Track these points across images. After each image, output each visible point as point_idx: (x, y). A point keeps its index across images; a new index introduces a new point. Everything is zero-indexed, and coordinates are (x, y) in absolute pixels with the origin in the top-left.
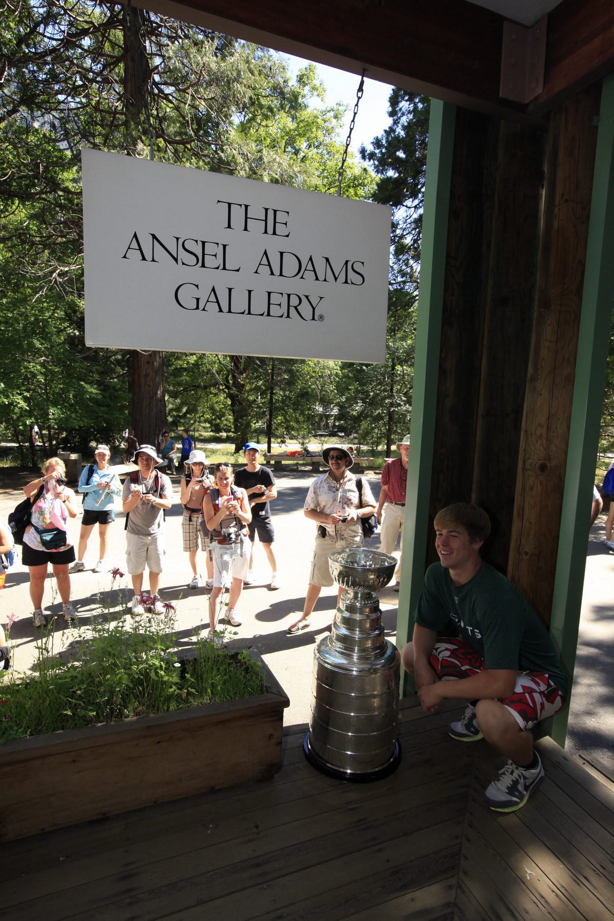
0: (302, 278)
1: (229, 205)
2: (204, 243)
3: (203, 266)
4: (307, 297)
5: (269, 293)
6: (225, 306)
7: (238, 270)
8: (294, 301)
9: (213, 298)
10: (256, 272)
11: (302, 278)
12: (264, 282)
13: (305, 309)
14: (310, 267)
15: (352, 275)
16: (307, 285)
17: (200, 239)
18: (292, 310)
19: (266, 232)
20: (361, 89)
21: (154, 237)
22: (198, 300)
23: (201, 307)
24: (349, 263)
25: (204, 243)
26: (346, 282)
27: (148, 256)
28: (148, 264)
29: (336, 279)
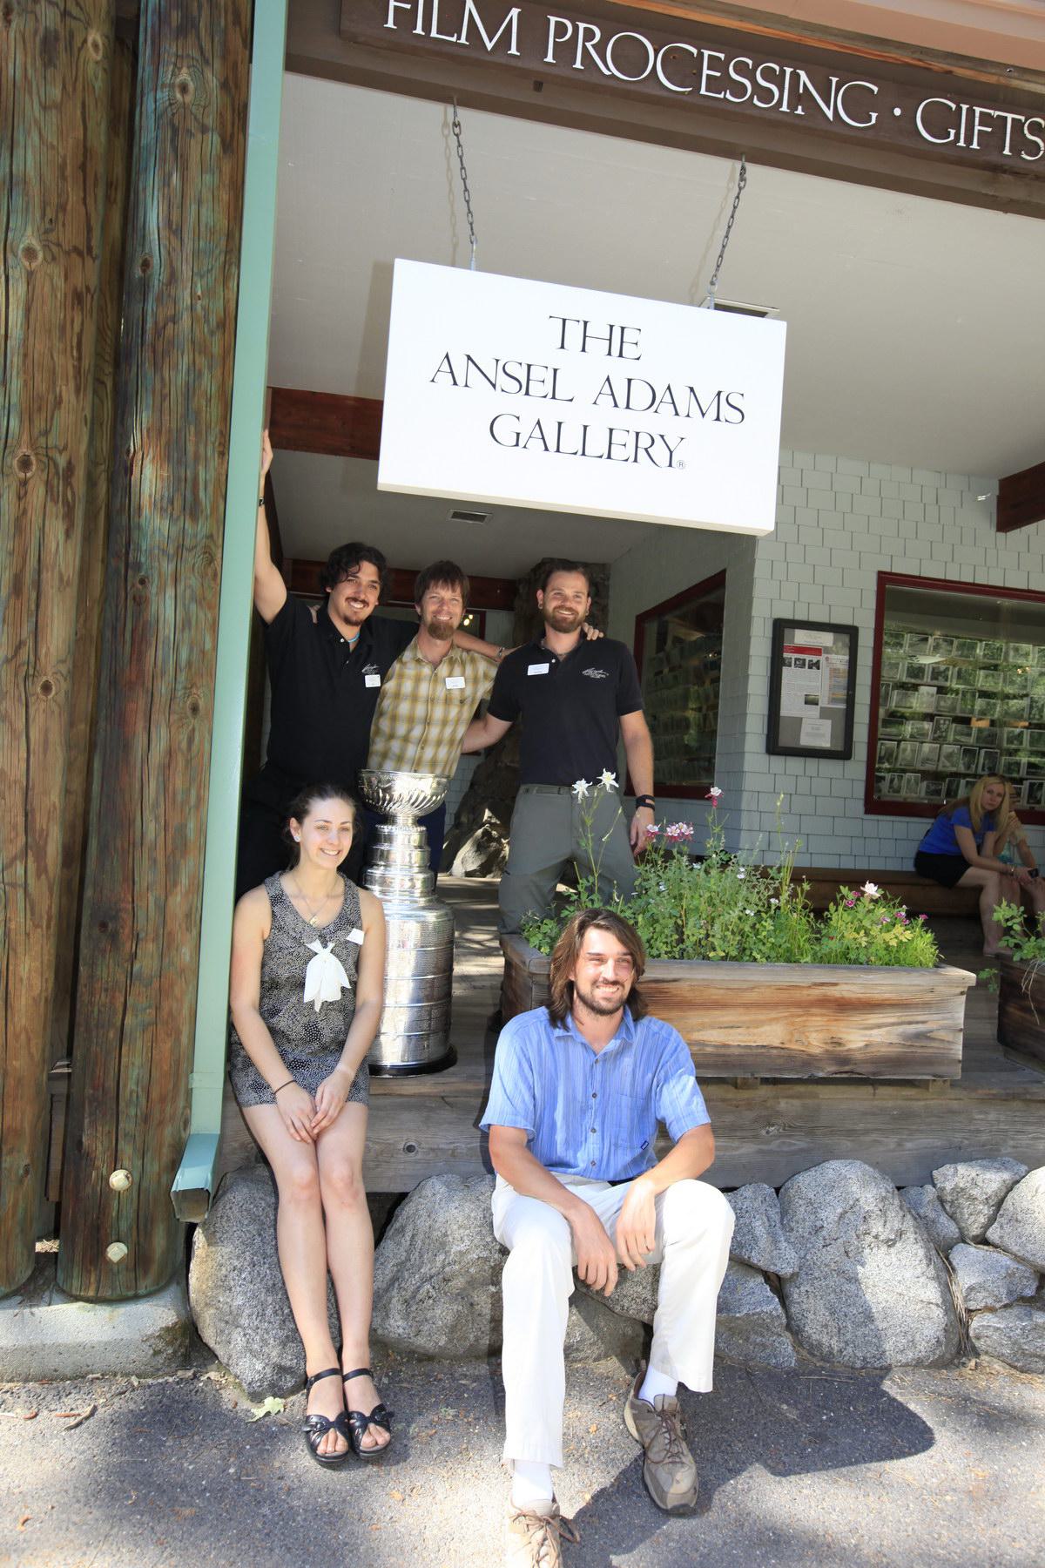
1: (564, 320)
2: (529, 366)
3: (527, 393)
4: (662, 436)
5: (611, 430)
7: (571, 400)
9: (537, 433)
12: (604, 416)
13: (659, 452)
14: (668, 398)
15: (726, 411)
16: (661, 422)
17: (525, 361)
18: (641, 453)
19: (609, 354)
20: (742, 179)
21: (469, 358)
22: (518, 434)
23: (522, 443)
25: (529, 366)
26: (718, 419)
27: (461, 380)
28: (460, 388)
29: (703, 415)
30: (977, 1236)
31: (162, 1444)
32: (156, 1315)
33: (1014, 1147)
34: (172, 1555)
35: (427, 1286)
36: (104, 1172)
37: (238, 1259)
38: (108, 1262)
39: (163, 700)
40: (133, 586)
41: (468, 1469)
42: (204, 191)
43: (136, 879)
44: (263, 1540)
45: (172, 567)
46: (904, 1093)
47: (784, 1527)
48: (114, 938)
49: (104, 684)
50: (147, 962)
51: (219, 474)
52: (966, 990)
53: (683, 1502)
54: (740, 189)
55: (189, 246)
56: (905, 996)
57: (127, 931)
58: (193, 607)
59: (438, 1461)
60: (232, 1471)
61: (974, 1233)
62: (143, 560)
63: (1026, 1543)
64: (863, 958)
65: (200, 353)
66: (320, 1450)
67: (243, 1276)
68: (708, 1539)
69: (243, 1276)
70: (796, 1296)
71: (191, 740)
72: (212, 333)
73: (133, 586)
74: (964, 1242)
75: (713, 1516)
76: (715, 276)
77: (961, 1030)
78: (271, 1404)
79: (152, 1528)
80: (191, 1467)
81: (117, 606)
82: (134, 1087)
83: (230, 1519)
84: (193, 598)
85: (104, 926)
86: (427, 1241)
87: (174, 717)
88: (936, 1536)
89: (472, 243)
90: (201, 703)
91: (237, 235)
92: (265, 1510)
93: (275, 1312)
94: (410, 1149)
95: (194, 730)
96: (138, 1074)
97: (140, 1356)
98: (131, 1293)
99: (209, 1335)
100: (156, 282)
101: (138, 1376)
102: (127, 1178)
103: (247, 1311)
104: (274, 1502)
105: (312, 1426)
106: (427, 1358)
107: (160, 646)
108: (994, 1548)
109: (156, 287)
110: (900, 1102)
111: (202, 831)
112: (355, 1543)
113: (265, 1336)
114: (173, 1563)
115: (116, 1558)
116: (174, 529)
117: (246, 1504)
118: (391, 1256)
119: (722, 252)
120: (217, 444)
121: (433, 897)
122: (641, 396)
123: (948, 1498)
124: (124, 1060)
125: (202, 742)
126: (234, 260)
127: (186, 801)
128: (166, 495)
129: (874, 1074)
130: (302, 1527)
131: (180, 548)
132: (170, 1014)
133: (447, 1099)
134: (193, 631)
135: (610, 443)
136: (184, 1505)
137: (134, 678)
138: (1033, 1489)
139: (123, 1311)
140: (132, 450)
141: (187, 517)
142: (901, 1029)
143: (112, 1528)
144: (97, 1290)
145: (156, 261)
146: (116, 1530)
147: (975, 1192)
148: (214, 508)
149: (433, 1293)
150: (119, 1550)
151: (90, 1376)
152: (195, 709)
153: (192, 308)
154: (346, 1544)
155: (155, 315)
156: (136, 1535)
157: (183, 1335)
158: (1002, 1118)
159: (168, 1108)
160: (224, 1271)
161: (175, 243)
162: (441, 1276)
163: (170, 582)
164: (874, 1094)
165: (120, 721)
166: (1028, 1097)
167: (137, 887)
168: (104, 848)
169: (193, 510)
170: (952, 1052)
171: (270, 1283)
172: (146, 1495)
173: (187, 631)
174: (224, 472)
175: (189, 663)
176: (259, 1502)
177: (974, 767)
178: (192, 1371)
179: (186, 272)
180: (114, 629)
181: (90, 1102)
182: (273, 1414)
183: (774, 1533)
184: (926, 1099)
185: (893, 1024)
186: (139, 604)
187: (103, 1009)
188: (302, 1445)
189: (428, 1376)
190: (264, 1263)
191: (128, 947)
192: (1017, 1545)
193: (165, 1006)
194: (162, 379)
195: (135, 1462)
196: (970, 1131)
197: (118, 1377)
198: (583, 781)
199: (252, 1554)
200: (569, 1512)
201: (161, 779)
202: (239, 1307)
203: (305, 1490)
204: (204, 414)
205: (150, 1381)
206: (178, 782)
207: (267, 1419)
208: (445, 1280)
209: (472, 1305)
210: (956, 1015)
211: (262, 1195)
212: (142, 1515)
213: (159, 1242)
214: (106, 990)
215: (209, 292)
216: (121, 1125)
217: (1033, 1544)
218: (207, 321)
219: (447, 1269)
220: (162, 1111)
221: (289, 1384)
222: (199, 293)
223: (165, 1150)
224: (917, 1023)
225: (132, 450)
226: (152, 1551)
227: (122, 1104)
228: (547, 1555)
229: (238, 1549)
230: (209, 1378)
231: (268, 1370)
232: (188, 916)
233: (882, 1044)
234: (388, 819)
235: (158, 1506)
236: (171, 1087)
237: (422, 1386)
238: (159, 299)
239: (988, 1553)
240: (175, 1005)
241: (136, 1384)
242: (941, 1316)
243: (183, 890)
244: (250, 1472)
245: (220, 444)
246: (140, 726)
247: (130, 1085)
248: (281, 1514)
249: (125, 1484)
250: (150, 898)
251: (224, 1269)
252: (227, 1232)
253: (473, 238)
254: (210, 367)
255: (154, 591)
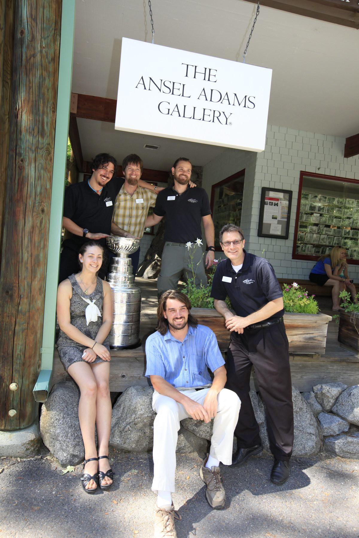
0: (222, 103)
1: (188, 65)
2: (174, 83)
3: (173, 94)
4: (224, 113)
5: (204, 109)
6: (182, 114)
7: (189, 97)
8: (217, 114)
9: (176, 109)
10: (198, 99)
11: (222, 103)
12: (202, 104)
14: (226, 98)
15: (248, 103)
16: (224, 107)
17: (172, 81)
18: (215, 118)
19: (205, 79)
20: (258, 11)
21: (151, 79)
22: (169, 110)
23: (170, 113)
24: (247, 97)
25: (174, 83)
26: (245, 106)
27: (147, 88)
28: (147, 91)
29: (239, 105)
30: (328, 410)
31: (28, 483)
32: (28, 435)
33: (342, 378)
34: (30, 524)
35: (128, 426)
36: (8, 384)
37: (58, 416)
38: (9, 417)
39: (30, 207)
40: (18, 162)
41: (142, 492)
42: (45, 2)
43: (20, 275)
44: (64, 519)
45: (33, 155)
46: (304, 359)
47: (256, 513)
48: (11, 296)
49: (7, 200)
50: (24, 306)
51: (53, 120)
52: (328, 322)
53: (220, 505)
54: (257, 15)
55: (39, 26)
56: (306, 324)
57: (16, 294)
58: (42, 171)
59: (131, 489)
60: (54, 493)
61: (327, 409)
62: (22, 152)
63: (342, 518)
64: (291, 310)
65: (44, 71)
66: (86, 488)
67: (60, 422)
68: (229, 518)
69: (60, 422)
70: (263, 431)
71: (41, 223)
72: (49, 63)
73: (18, 162)
74: (323, 412)
75: (230, 509)
76: (246, 50)
77: (326, 337)
78: (70, 468)
79: (23, 514)
80: (38, 492)
81: (12, 170)
82: (19, 353)
83: (53, 511)
84: (42, 168)
85: (7, 292)
86: (129, 410)
87: (35, 214)
88: (310, 516)
89: (153, 32)
90: (45, 209)
91: (59, 23)
92: (66, 507)
93: (72, 435)
94: (123, 376)
95: (42, 219)
96: (21, 348)
97: (22, 450)
98: (18, 428)
99: (47, 443)
100: (27, 40)
101: (20, 458)
102: (16, 386)
103: (61, 435)
104: (69, 504)
105: (84, 478)
106: (129, 452)
107: (29, 186)
108: (331, 521)
109: (26, 42)
110: (303, 362)
111: (46, 257)
112: (99, 520)
113: (68, 444)
114: (30, 527)
115: (9, 525)
116: (35, 141)
117: (59, 505)
118: (115, 415)
119: (249, 41)
120: (52, 107)
121: (133, 284)
122: (216, 97)
123: (315, 503)
124: (15, 343)
125: (45, 223)
126: (58, 33)
127: (39, 246)
128: (31, 127)
129: (294, 352)
130: (79, 513)
131: (37, 148)
132: (33, 326)
133: (137, 359)
134: (42, 181)
135: (204, 115)
136: (35, 505)
137: (19, 198)
138: (345, 499)
139: (15, 434)
140: (18, 108)
141: (40, 136)
142: (304, 336)
143: (8, 514)
144: (5, 427)
145: (26, 31)
146: (9, 515)
147: (328, 395)
148: (51, 133)
149: (130, 428)
150: (9, 522)
151: (2, 458)
152: (43, 211)
153: (41, 51)
154: (95, 520)
155: (26, 54)
156: (16, 517)
157: (38, 443)
158: (339, 368)
159: (32, 361)
160: (53, 420)
161: (34, 24)
162: (133, 423)
163: (33, 161)
164: (293, 359)
165: (14, 214)
166: (348, 361)
167: (20, 278)
168: (7, 263)
169: (42, 133)
170: (322, 344)
171: (70, 424)
172: (21, 502)
173: (40, 180)
174: (54, 119)
175: (41, 193)
176: (64, 504)
177: (332, 243)
178: (41, 456)
179: (38, 37)
180: (11, 179)
181: (2, 358)
182: (70, 472)
183: (252, 516)
184: (312, 361)
185: (301, 334)
186: (21, 169)
187: (7, 323)
188: (80, 484)
189: (128, 458)
190: (68, 417)
191: (16, 300)
192: (339, 520)
193: (31, 323)
194: (29, 80)
195: (17, 490)
196: (327, 373)
197: (13, 458)
198: (190, 242)
199: (60, 524)
200: (177, 508)
201: (29, 237)
202: (58, 433)
203: (81, 500)
204: (46, 95)
205: (25, 459)
206: (36, 238)
207: (68, 474)
208: (135, 424)
209: (145, 433)
210: (324, 331)
211: (68, 393)
212: (19, 510)
213: (29, 409)
214: (8, 316)
215: (48, 45)
216: (14, 367)
217: (345, 519)
218: (47, 57)
219: (136, 420)
220: (30, 362)
221: (77, 461)
222: (44, 46)
223: (31, 376)
224: (310, 334)
225: (18, 108)
226: (22, 523)
227: (14, 359)
228: (169, 525)
229: (55, 522)
230: (47, 459)
231: (69, 456)
232: (40, 289)
233: (297, 341)
234: (117, 255)
235: (25, 506)
236: (33, 353)
237: (126, 462)
238: (28, 47)
239: (329, 522)
240: (35, 323)
241: (19, 461)
242: (314, 438)
243: (38, 279)
244: (61, 493)
245: (53, 108)
246: (21, 216)
247: (18, 351)
248: (71, 509)
249: (13, 498)
250: (25, 282)
251: (53, 419)
252: (54, 406)
253: (153, 30)
254: (49, 77)
255: (27, 164)
